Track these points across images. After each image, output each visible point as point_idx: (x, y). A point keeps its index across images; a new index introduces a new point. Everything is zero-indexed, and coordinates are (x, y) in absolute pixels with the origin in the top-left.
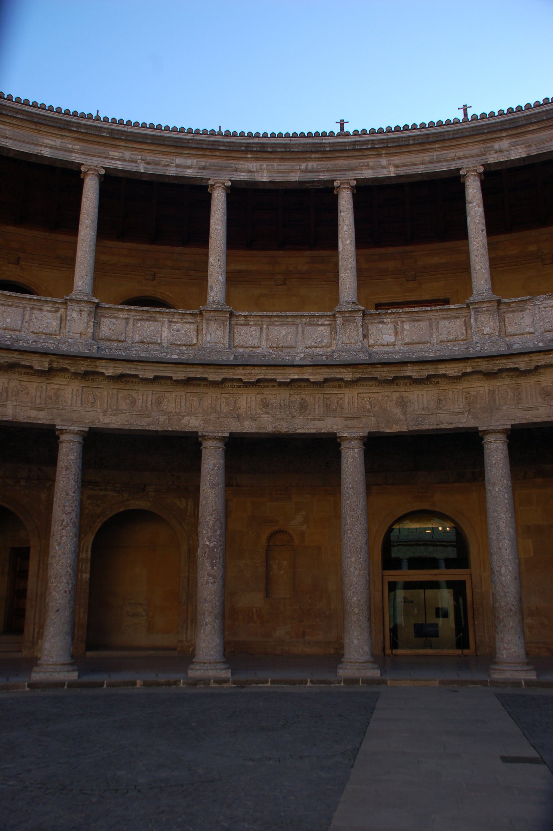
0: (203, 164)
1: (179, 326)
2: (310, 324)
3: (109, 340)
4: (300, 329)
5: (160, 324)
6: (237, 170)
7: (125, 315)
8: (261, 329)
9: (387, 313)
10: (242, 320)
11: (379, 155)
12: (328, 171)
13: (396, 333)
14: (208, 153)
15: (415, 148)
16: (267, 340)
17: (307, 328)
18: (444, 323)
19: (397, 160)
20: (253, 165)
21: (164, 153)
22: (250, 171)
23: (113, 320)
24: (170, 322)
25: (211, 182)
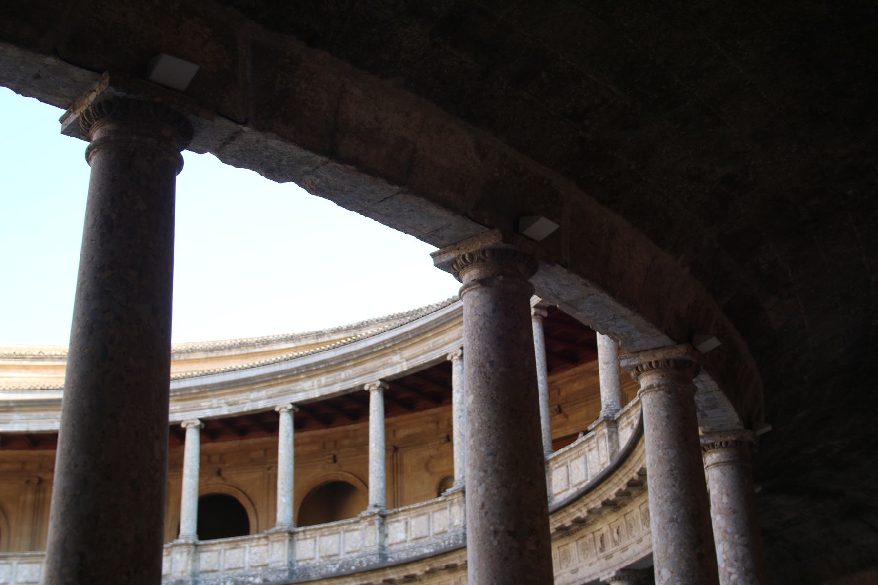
0: (270, 393)
1: (255, 550)
2: (347, 531)
3: (207, 572)
4: (342, 536)
5: (242, 550)
6: (295, 392)
7: (218, 547)
8: (315, 541)
9: (399, 512)
10: (301, 536)
11: (394, 352)
12: (360, 376)
13: (406, 530)
14: (273, 383)
15: (417, 340)
16: (320, 551)
17: (347, 535)
18: (437, 515)
19: (407, 353)
20: (307, 384)
21: (241, 392)
22: (304, 391)
23: (208, 554)
24: (251, 546)
25: (277, 409)
